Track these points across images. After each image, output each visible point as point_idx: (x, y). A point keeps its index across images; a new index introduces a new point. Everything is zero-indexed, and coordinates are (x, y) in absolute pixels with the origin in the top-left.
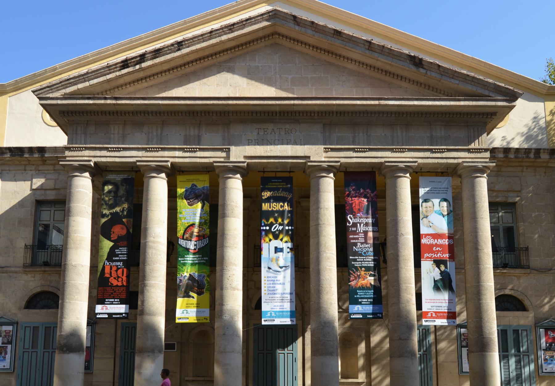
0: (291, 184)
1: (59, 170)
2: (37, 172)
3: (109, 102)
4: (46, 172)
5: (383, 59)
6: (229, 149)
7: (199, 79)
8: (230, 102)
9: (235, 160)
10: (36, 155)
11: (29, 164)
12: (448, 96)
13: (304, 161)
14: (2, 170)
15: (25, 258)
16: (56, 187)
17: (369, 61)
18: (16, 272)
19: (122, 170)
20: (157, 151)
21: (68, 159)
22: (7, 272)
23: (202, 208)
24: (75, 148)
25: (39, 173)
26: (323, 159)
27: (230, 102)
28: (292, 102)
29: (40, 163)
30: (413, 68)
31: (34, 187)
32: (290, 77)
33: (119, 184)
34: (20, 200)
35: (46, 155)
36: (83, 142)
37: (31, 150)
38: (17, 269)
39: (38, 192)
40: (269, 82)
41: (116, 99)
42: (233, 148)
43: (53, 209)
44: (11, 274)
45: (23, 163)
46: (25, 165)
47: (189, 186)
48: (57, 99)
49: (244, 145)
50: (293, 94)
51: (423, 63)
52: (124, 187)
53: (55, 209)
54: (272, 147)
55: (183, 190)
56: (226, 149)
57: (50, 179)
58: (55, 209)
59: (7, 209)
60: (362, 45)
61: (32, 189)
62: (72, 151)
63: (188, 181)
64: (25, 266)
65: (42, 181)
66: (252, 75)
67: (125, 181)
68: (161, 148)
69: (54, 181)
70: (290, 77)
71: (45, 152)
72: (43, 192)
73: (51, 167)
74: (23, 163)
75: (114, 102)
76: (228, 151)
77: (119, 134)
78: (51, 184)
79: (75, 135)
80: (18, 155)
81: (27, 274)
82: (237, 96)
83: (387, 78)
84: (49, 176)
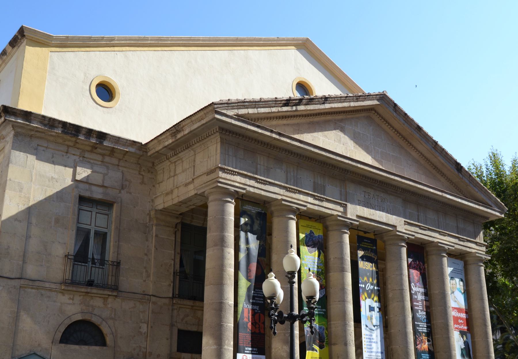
0: (376, 247)
1: (107, 163)
2: (81, 159)
3: (274, 136)
4: (92, 161)
5: (440, 158)
6: (346, 205)
7: (322, 130)
8: (359, 165)
9: (351, 217)
10: (93, 140)
11: (74, 147)
12: (465, 197)
13: (391, 229)
14: (38, 145)
15: (65, 271)
16: (105, 185)
17: (428, 155)
18: (51, 290)
19: (248, 200)
20: (295, 193)
21: (221, 180)
22: (38, 288)
23: (319, 256)
24: (229, 170)
25: (84, 162)
26: (404, 231)
27: (359, 165)
28: (392, 177)
29: (89, 148)
30: (456, 172)
31: (78, 178)
32: (380, 150)
33: (254, 217)
34: (58, 190)
35: (106, 143)
36: (234, 167)
37: (90, 132)
38: (53, 286)
39: (81, 185)
40: (367, 150)
41: (280, 134)
42: (349, 205)
43: (95, 210)
44: (43, 292)
45: (67, 143)
46: (68, 146)
47: (308, 232)
48: (231, 117)
49: (356, 204)
50: (382, 166)
51: (462, 170)
52: (258, 222)
53: (97, 211)
54: (372, 211)
55: (304, 235)
56: (344, 204)
57: (98, 172)
58: (97, 211)
59: (41, 199)
60: (431, 143)
61: (74, 179)
62: (225, 173)
63: (308, 226)
64: (64, 282)
65: (88, 172)
66: (357, 139)
67: (259, 214)
68: (299, 191)
69: (102, 175)
70: (380, 150)
71: (104, 140)
72: (87, 186)
73: (100, 158)
74: (67, 143)
75: (277, 137)
76: (345, 207)
77: (264, 166)
78: (98, 179)
79: (227, 156)
80: (71, 134)
81: (63, 294)
82: (348, 156)
83: (434, 171)
84: (96, 168)
